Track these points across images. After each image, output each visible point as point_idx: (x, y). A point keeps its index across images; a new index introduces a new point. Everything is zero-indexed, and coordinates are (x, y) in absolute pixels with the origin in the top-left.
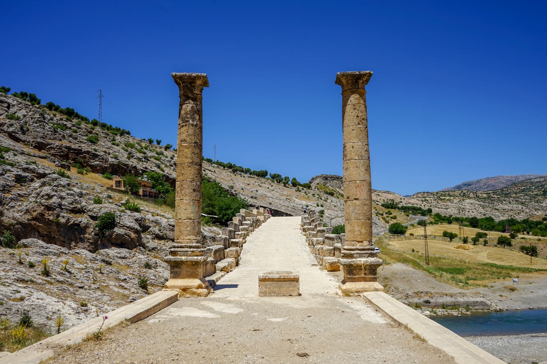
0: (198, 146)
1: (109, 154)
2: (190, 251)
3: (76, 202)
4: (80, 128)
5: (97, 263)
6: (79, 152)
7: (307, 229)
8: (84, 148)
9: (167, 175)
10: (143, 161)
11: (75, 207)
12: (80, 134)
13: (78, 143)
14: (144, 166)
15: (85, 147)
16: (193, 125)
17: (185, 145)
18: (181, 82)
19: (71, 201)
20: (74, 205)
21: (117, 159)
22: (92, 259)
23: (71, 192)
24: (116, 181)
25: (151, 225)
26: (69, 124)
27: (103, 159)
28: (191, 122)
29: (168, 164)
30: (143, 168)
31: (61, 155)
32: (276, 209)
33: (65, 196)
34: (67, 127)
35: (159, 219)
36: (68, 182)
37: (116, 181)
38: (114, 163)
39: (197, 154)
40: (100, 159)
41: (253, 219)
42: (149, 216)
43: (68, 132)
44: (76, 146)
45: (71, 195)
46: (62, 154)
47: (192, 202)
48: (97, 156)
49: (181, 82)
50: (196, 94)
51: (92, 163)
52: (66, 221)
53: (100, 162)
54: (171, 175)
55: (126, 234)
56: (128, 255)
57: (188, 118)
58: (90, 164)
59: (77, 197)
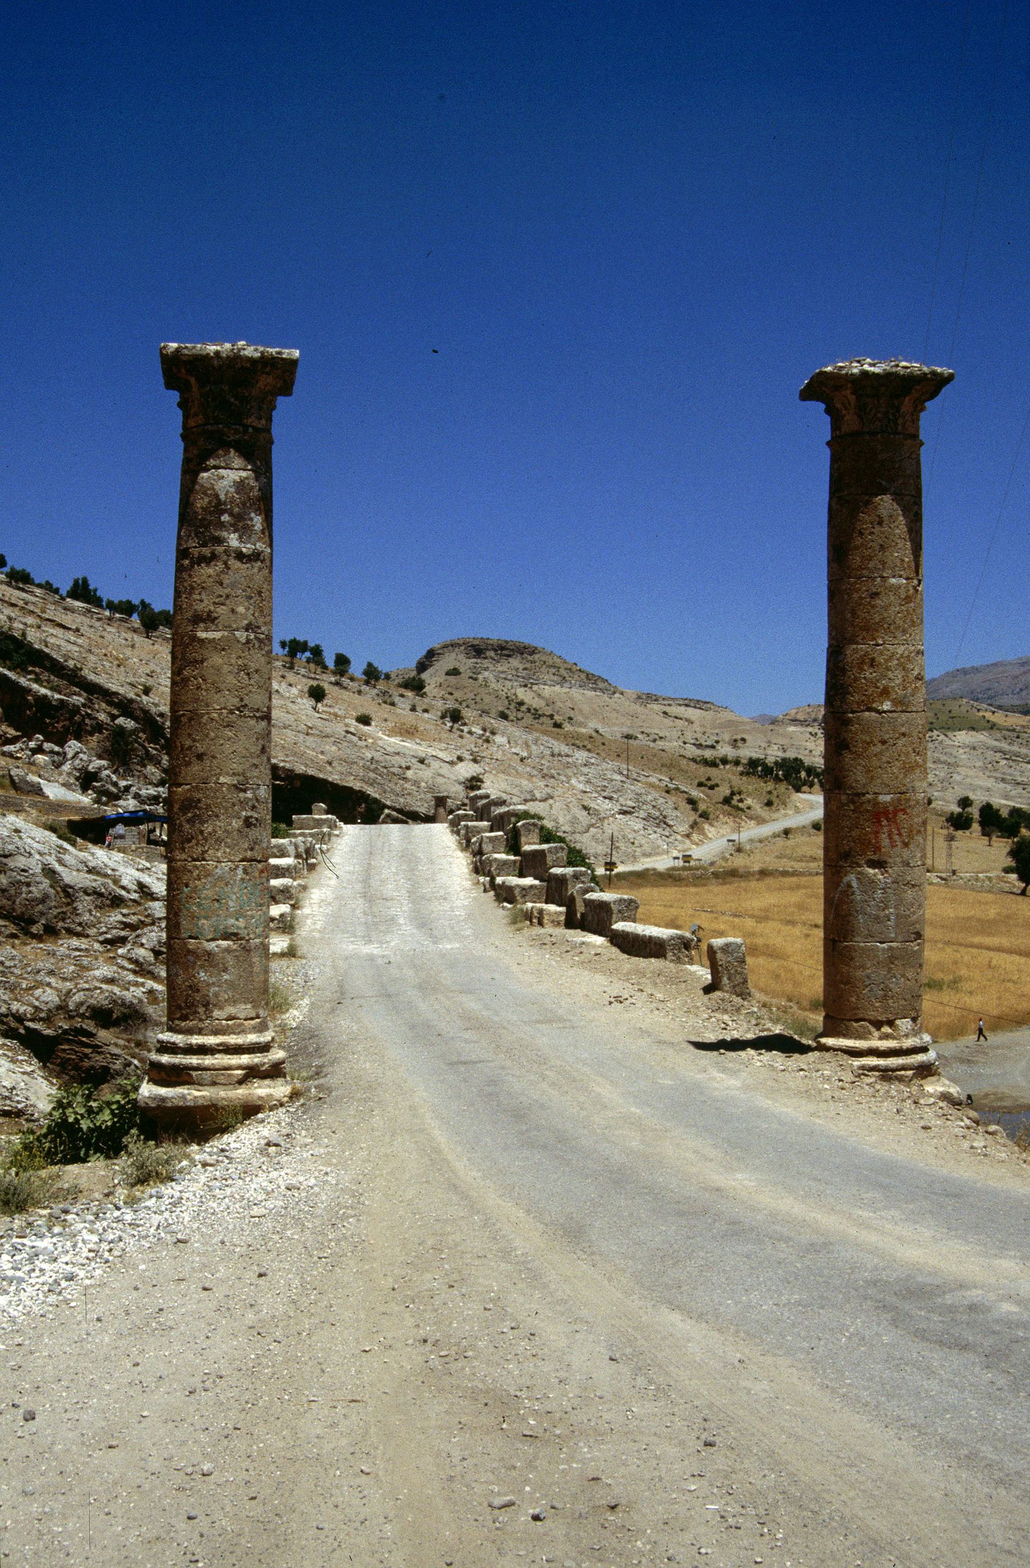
0: (260, 641)
2: (240, 1067)
7: (517, 892)
16: (240, 556)
17: (210, 635)
18: (193, 380)
28: (233, 540)
39: (257, 671)
41: (296, 847)
47: (240, 871)
49: (193, 380)
50: (254, 428)
57: (222, 525)
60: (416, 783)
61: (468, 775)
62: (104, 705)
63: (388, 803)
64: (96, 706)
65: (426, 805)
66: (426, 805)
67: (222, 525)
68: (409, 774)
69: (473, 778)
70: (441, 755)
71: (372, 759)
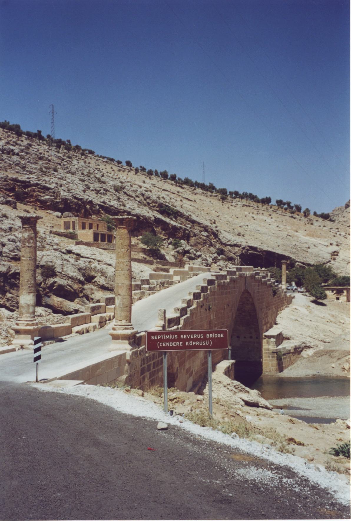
1: (61, 186)
3: (17, 250)
4: (29, 154)
5: (12, 321)
6: (26, 184)
8: (33, 179)
9: (129, 210)
10: (101, 194)
11: (16, 255)
12: (28, 162)
13: (26, 174)
14: (102, 200)
15: (33, 179)
16: (28, 247)
19: (12, 248)
20: (15, 252)
21: (71, 193)
22: (8, 317)
23: (13, 237)
24: (64, 222)
25: (96, 275)
26: (16, 149)
27: (54, 193)
28: (27, 244)
29: (134, 195)
30: (101, 202)
31: (7, 188)
32: (269, 249)
33: (6, 242)
34: (15, 153)
35: (106, 269)
36: (10, 226)
37: (64, 222)
38: (66, 197)
40: (50, 192)
42: (95, 264)
43: (15, 158)
44: (24, 178)
45: (14, 241)
46: (8, 187)
48: (48, 189)
51: (42, 198)
52: (7, 269)
53: (51, 196)
54: (134, 209)
55: (68, 285)
56: (43, 313)
57: (25, 242)
58: (39, 198)
59: (18, 244)
60: (312, 254)
61: (334, 250)
62: (198, 228)
63: (299, 260)
64: (195, 228)
65: (314, 261)
66: (314, 261)
67: (25, 242)
68: (309, 250)
69: (335, 252)
70: (323, 243)
71: (295, 245)
